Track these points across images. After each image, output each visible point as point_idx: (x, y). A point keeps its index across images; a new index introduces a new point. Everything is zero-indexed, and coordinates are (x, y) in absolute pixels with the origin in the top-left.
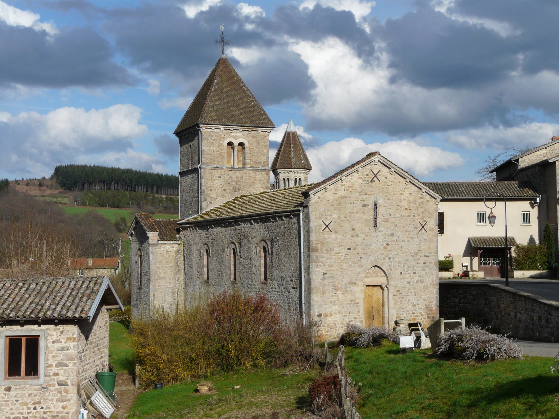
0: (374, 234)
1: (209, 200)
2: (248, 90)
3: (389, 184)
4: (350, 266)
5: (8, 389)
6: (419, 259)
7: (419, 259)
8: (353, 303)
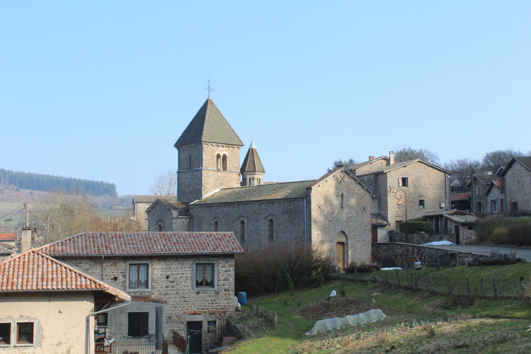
1: (206, 190)
5: (198, 293)
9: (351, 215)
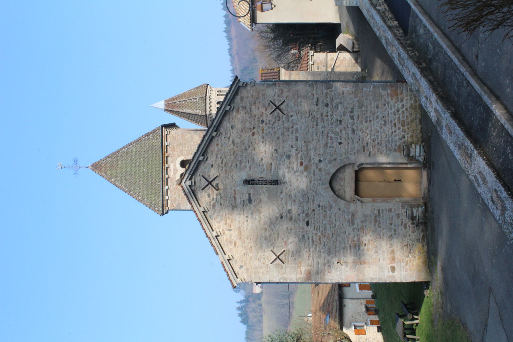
2: (123, 148)
3: (220, 161)
4: (330, 223)
6: (322, 114)
7: (322, 114)
9: (293, 151)
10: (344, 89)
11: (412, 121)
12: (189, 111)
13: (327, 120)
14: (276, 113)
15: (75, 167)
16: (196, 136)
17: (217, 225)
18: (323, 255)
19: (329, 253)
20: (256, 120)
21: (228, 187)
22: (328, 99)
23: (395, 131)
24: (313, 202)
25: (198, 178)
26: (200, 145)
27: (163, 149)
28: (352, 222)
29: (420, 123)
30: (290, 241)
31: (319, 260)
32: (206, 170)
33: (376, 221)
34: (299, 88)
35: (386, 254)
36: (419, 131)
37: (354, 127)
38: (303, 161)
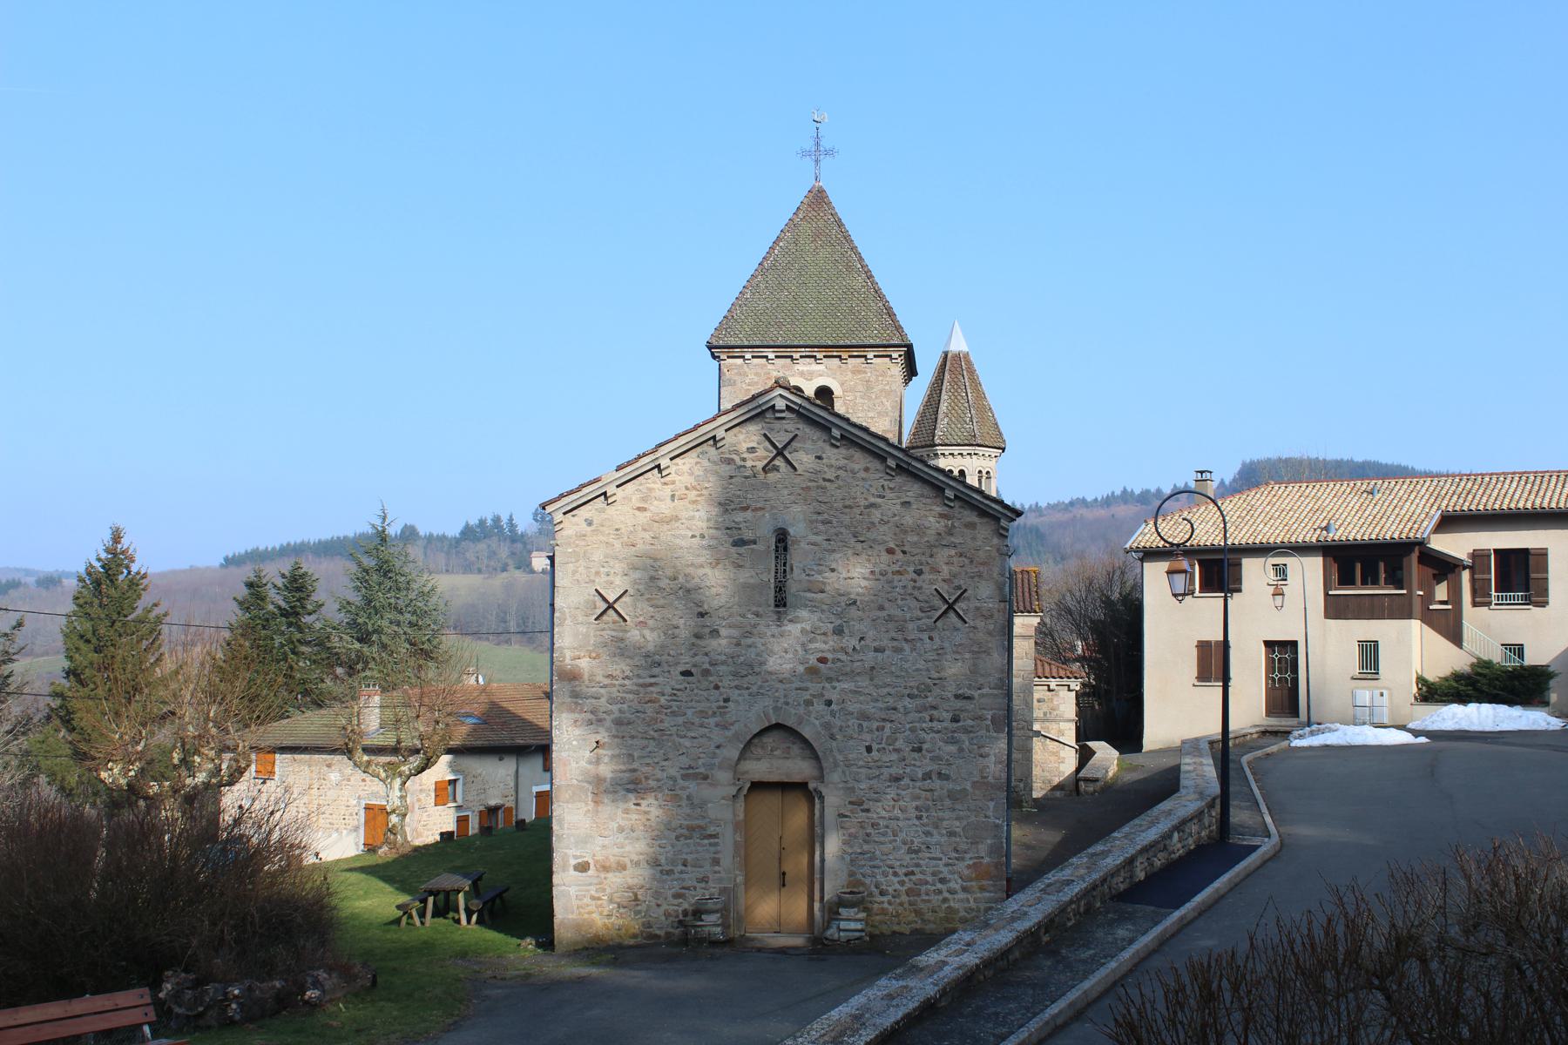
0: (774, 630)
2: (861, 259)
4: (688, 725)
7: (934, 708)
8: (696, 835)
10: (993, 758)
11: (918, 912)
12: (943, 407)
13: (921, 720)
14: (937, 602)
15: (818, 152)
16: (887, 423)
17: (686, 468)
18: (615, 708)
19: (618, 722)
20: (923, 559)
21: (771, 494)
22: (970, 722)
23: (895, 874)
24: (737, 687)
25: (792, 425)
26: (866, 430)
27: (857, 349)
28: (689, 774)
29: (915, 932)
30: (647, 633)
31: (603, 700)
32: (808, 445)
33: (691, 829)
34: (996, 655)
35: (616, 851)
36: (896, 928)
37: (906, 781)
38: (829, 665)
